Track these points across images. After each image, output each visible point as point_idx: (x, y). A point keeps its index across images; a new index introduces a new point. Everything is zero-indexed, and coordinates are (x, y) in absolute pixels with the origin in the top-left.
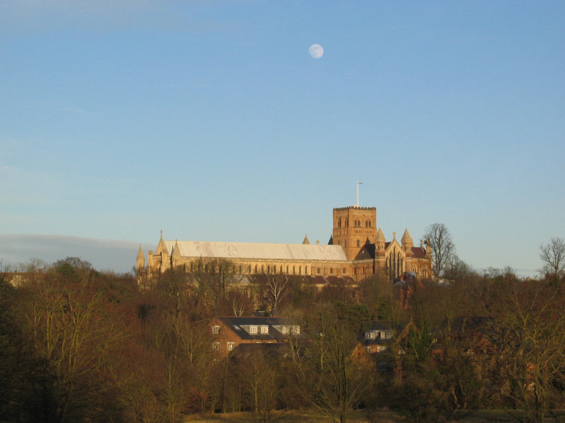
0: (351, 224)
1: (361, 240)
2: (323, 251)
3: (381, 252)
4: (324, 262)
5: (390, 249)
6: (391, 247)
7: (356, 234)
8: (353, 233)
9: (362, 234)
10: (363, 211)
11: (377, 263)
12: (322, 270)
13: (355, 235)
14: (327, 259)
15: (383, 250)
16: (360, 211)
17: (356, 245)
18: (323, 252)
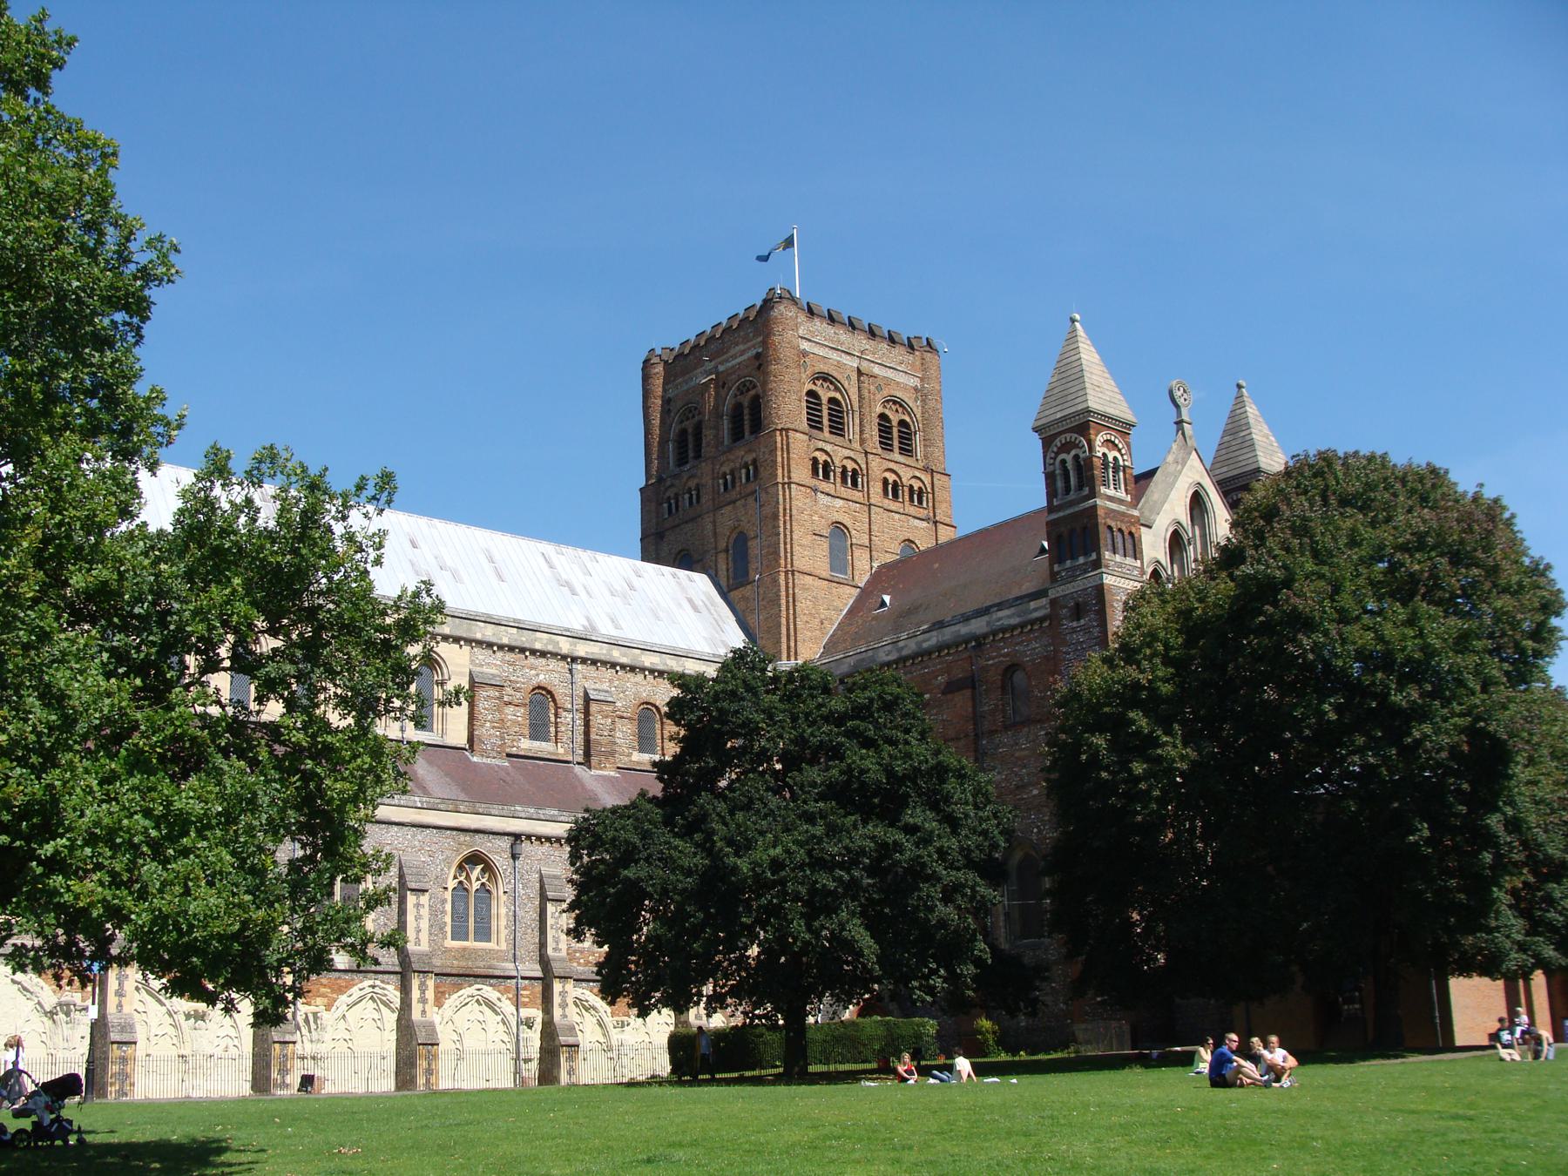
0: (789, 408)
1: (860, 537)
2: (579, 589)
3: (1111, 513)
4: (582, 650)
5: (1166, 506)
6: (1173, 495)
7: (824, 486)
8: (801, 473)
9: (857, 495)
10: (861, 342)
12: (566, 717)
13: (815, 491)
14: (606, 629)
15: (1121, 502)
16: (843, 336)
17: (823, 568)
18: (574, 593)
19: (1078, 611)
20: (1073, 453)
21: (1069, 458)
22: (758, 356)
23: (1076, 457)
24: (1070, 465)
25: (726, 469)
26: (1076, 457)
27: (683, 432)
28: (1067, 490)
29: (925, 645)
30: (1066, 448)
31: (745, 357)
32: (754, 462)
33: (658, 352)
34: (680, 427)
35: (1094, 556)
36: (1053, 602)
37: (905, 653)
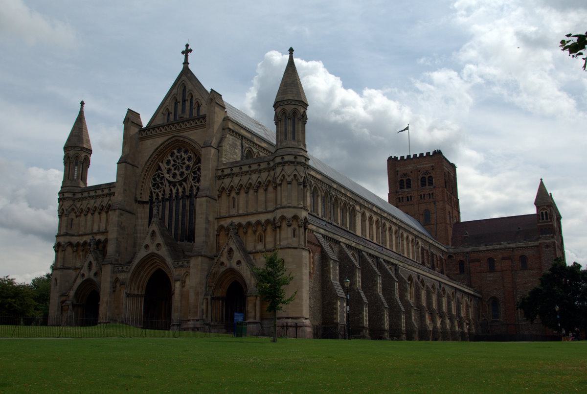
11: (547, 246)
19: (547, 246)
20: (545, 211)
21: (544, 212)
22: (432, 166)
23: (546, 212)
24: (544, 214)
25: (422, 194)
26: (546, 212)
27: (402, 180)
28: (543, 219)
29: (495, 248)
30: (543, 209)
31: (428, 165)
32: (432, 193)
33: (393, 157)
34: (401, 179)
35: (552, 235)
36: (540, 244)
37: (489, 249)
